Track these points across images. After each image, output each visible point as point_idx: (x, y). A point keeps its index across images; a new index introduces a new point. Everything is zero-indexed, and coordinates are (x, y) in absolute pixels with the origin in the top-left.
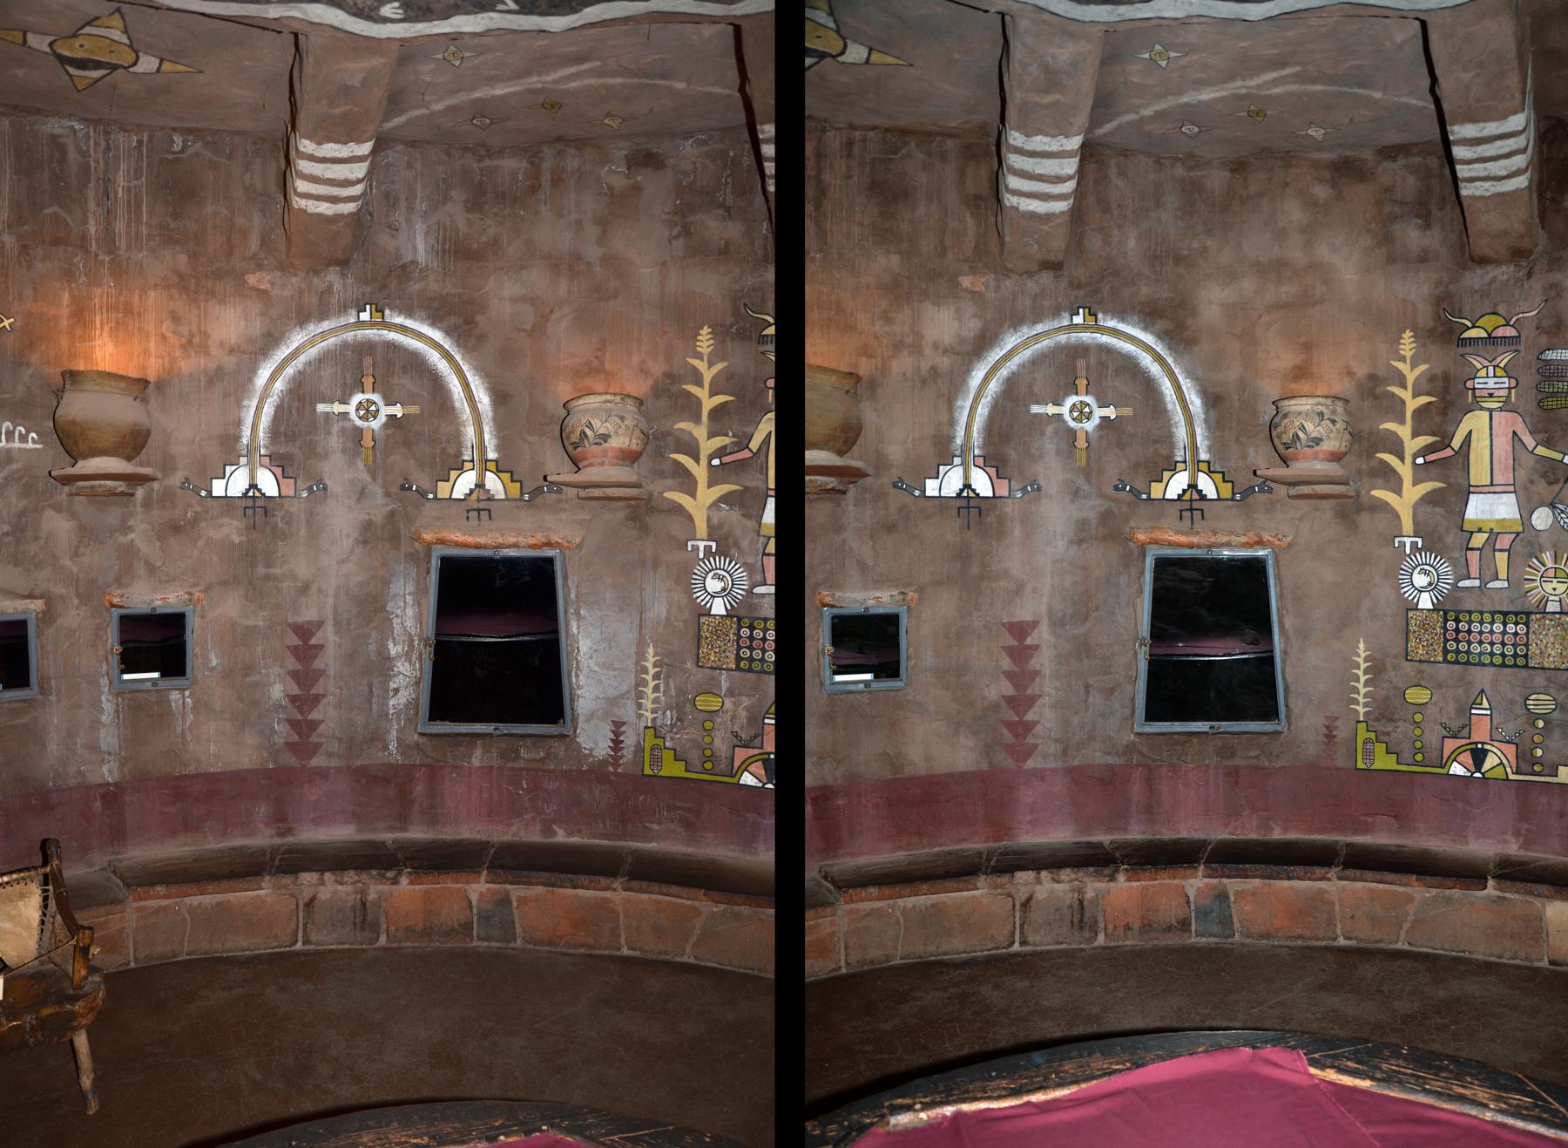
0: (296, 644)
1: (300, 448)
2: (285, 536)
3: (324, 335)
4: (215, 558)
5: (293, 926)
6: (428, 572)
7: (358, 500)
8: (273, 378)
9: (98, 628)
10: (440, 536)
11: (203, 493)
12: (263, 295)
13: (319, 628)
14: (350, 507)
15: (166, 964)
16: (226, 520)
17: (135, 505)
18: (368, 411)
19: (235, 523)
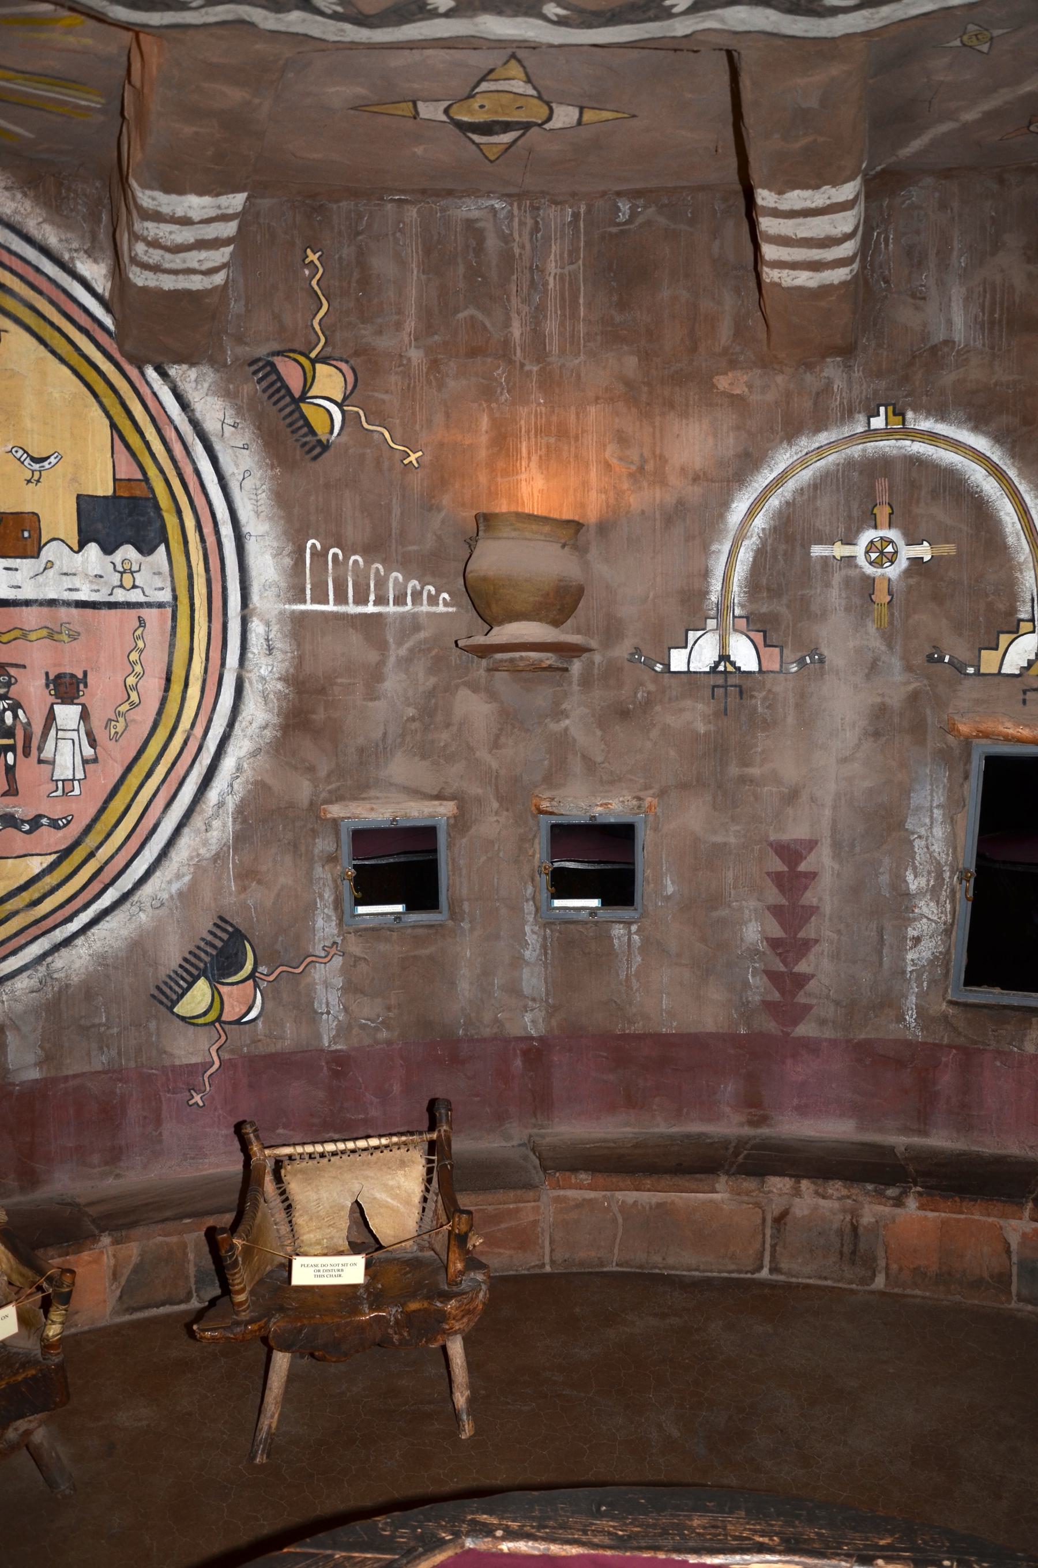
0: (780, 869)
1: (788, 607)
2: (767, 725)
3: (820, 452)
4: (672, 753)
5: (757, 1246)
6: (966, 777)
7: (868, 677)
8: (751, 513)
9: (522, 839)
10: (983, 727)
11: (659, 667)
12: (737, 402)
13: (811, 849)
14: (856, 686)
15: (591, 1273)
16: (688, 703)
17: (570, 683)
18: (882, 554)
19: (700, 706)
